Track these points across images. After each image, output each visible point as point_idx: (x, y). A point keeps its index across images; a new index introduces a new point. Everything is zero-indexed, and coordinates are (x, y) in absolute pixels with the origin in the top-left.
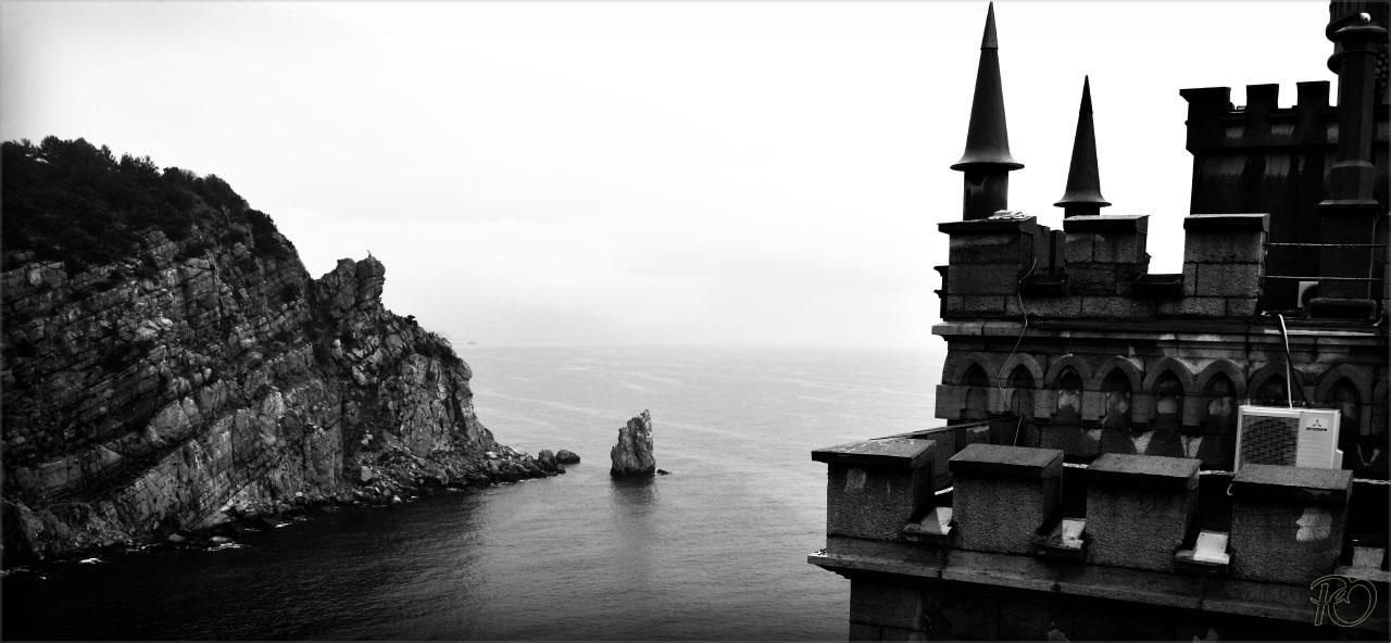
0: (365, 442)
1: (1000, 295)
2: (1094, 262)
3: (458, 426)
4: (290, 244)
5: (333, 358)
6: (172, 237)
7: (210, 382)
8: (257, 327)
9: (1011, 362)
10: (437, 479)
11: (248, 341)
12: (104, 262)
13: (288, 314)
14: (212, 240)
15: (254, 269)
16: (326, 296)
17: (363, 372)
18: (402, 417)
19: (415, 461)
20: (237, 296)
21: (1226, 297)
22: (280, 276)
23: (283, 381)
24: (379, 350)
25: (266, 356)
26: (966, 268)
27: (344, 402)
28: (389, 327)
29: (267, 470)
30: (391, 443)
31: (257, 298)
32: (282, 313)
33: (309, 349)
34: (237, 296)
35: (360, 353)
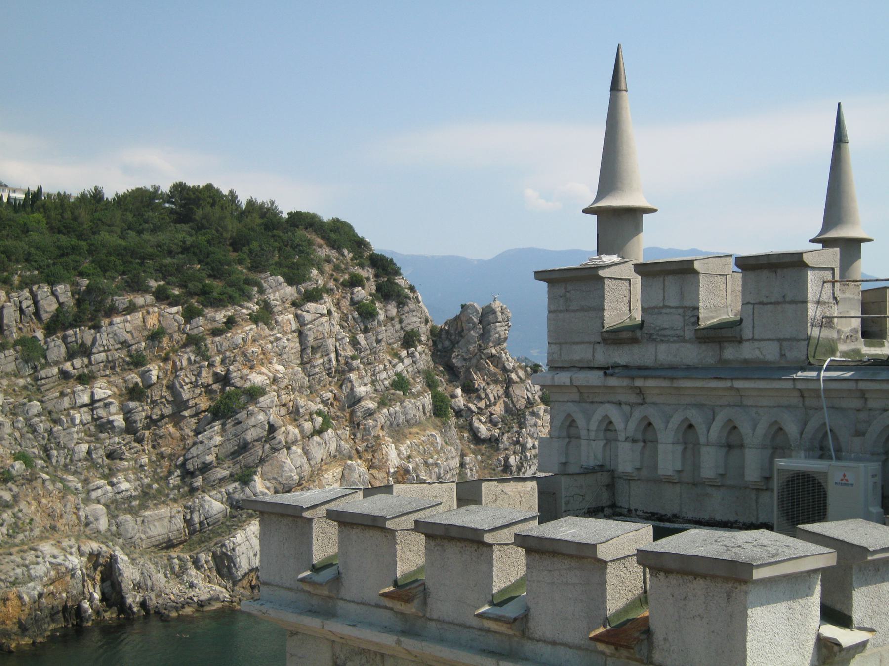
1: (590, 343)
2: (665, 307)
4: (412, 289)
6: (290, 282)
7: (319, 432)
8: (374, 375)
9: (599, 413)
12: (218, 304)
14: (331, 284)
16: (447, 343)
20: (354, 343)
21: (779, 340)
22: (401, 321)
23: (397, 431)
26: (561, 315)
27: (462, 456)
31: (375, 345)
32: (401, 360)
33: (427, 399)
34: (354, 343)
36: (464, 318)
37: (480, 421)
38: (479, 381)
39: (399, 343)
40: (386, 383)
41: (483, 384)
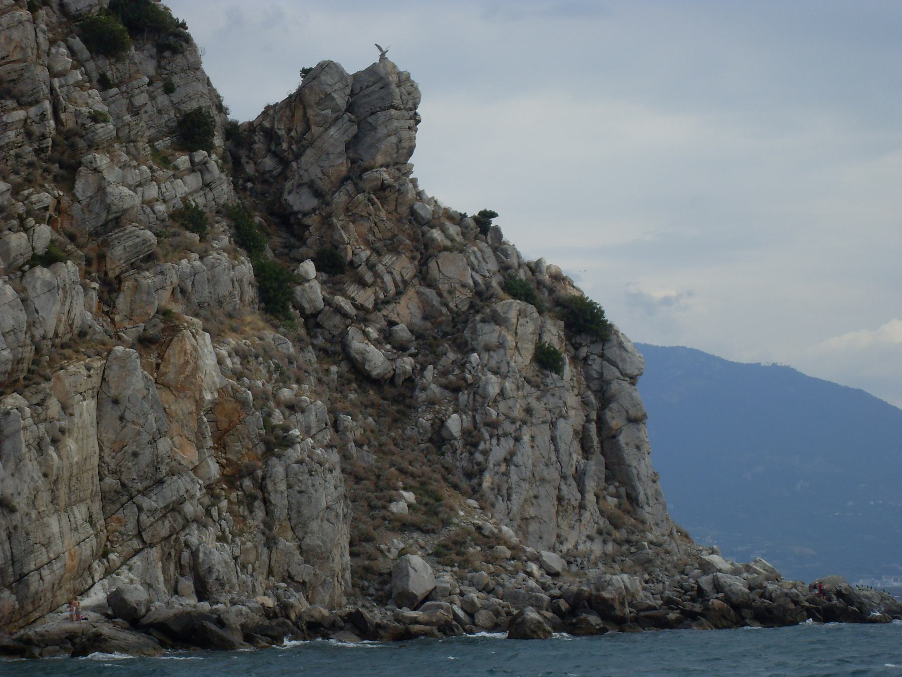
0: (399, 508)
3: (617, 496)
5: (298, 306)
10: (604, 600)
13: (194, 181)
16: (269, 163)
17: (377, 343)
18: (486, 453)
19: (537, 559)
24: (411, 292)
28: (436, 234)
29: (187, 523)
30: (465, 513)
31: (127, 118)
35: (366, 298)
36: (311, 99)
37: (366, 334)
38: (354, 245)
39: (168, 140)
41: (365, 254)
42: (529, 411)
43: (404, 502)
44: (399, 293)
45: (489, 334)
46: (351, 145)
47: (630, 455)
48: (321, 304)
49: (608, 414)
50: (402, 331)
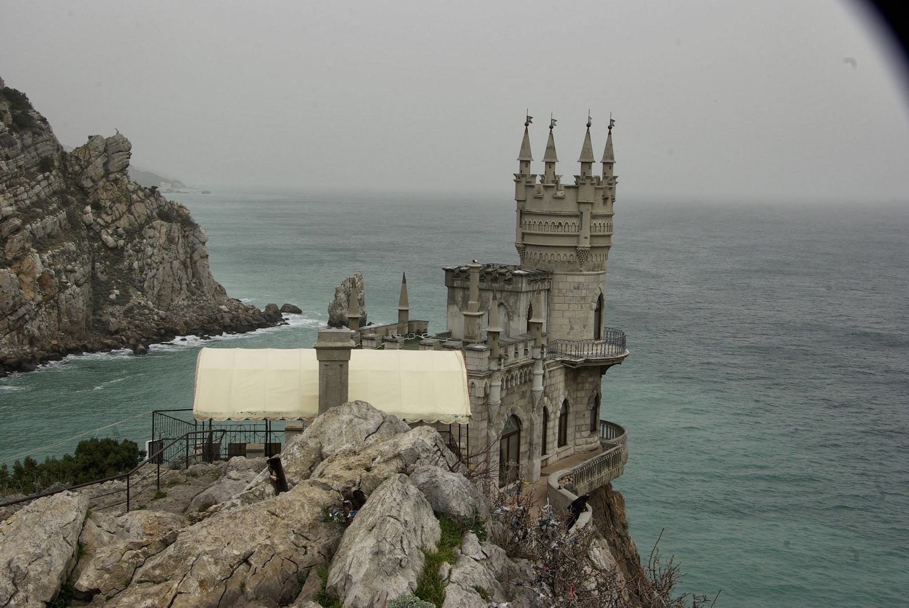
0: (113, 297)
4: (44, 120)
8: (15, 195)
11: (10, 209)
15: (11, 144)
16: (77, 168)
17: (112, 235)
18: (146, 275)
19: (157, 314)
22: (36, 149)
23: (41, 244)
24: (125, 216)
25: (25, 222)
27: (94, 262)
28: (134, 196)
29: (26, 322)
32: (39, 183)
33: (63, 215)
35: (109, 219)
39: (35, 168)
40: (28, 202)
42: (163, 259)
43: (115, 294)
44: (121, 217)
45: (151, 232)
46: (105, 164)
47: (200, 269)
48: (92, 221)
49: (194, 255)
50: (120, 230)
